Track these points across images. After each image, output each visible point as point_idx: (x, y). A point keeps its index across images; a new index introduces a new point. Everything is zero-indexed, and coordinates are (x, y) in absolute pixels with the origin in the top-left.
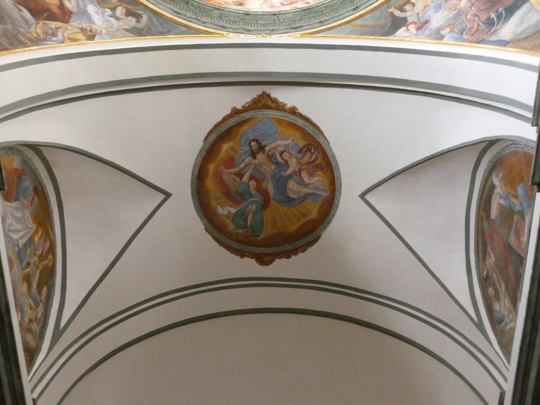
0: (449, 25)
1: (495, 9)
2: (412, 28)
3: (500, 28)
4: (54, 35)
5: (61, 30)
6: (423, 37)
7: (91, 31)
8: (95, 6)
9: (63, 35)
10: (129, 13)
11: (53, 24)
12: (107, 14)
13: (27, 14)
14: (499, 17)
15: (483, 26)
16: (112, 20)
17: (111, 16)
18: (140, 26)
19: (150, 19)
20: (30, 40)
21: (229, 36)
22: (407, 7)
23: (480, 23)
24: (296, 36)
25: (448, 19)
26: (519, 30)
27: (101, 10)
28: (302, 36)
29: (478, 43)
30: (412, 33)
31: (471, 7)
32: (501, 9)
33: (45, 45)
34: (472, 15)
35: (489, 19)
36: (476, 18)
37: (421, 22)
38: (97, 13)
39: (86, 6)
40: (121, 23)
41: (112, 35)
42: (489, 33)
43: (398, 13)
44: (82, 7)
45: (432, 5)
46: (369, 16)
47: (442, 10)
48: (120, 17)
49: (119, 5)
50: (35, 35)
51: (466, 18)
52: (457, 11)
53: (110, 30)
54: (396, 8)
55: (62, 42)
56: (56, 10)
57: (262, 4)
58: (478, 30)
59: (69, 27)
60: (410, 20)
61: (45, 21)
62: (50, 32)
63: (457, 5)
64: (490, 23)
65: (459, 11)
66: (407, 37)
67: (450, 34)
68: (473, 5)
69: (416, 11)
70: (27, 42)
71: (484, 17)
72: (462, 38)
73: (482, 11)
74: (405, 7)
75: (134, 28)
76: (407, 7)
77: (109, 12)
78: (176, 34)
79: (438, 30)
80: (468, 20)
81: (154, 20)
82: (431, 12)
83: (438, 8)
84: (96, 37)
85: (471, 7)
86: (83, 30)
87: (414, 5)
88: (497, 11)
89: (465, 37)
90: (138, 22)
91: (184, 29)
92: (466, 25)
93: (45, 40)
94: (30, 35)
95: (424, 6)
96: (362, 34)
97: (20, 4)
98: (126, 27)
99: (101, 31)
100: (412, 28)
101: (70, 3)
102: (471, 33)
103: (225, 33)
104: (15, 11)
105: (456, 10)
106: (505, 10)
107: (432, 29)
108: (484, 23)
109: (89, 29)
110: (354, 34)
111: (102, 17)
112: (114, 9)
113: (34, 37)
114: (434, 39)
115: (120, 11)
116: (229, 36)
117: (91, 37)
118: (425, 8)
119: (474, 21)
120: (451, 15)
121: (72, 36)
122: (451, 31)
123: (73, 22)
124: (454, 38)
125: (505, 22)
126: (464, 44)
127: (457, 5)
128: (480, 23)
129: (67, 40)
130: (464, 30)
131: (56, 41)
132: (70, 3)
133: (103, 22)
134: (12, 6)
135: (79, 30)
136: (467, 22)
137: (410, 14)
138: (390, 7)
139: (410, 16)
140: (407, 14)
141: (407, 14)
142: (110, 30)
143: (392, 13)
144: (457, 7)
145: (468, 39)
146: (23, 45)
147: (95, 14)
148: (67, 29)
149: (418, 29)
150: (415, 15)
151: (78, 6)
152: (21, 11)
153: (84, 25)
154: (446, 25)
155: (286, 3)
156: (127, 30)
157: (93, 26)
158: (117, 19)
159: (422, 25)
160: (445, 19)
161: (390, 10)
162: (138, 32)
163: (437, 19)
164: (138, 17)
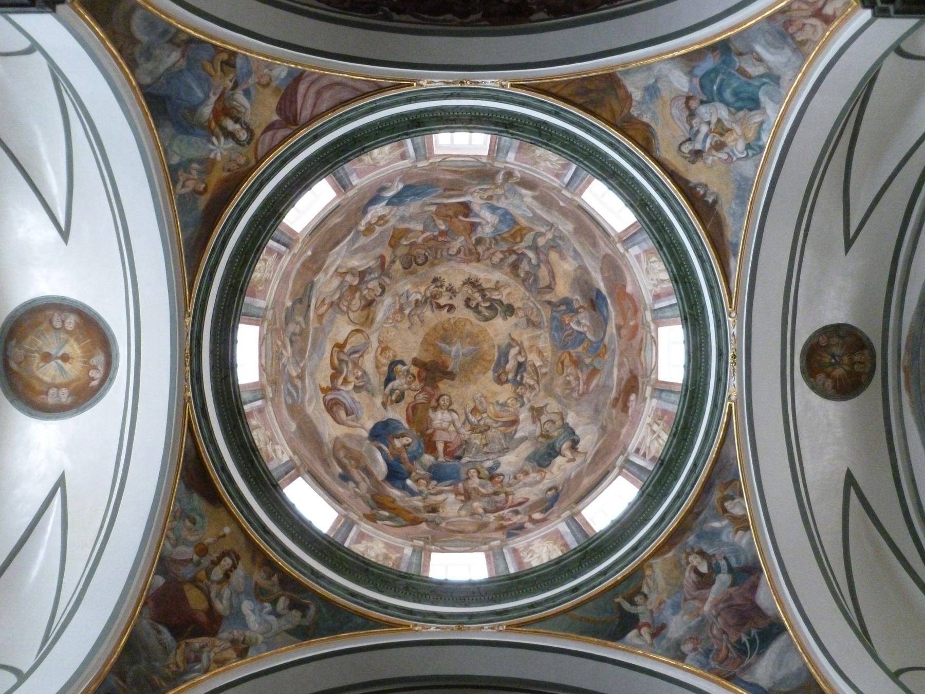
0: (691, 638)
1: (746, 628)
2: (645, 631)
3: (756, 662)
4: (198, 660)
5: (207, 649)
6: (659, 651)
7: (243, 642)
8: (252, 601)
9: (209, 656)
10: (294, 605)
11: (197, 642)
12: (265, 610)
13: (167, 635)
14: (752, 641)
15: (733, 654)
16: (272, 618)
17: (270, 613)
18: (306, 622)
19: (318, 611)
20: (167, 679)
21: (417, 628)
22: (638, 599)
23: (730, 646)
24: (501, 628)
25: (689, 628)
26: (779, 675)
27: (259, 606)
28: (510, 628)
29: (728, 679)
30: (645, 641)
31: (716, 617)
32: (754, 632)
33: (185, 681)
34: (718, 630)
35: (739, 641)
36: (724, 636)
37: (656, 625)
38: (253, 611)
39: (240, 603)
40: (282, 621)
41: (271, 645)
42: (742, 666)
43: (626, 606)
44: (235, 605)
45: (669, 601)
46: (591, 604)
47: (682, 612)
48: (282, 612)
49: (281, 595)
50: (173, 668)
51: (711, 631)
52: (700, 618)
53: (269, 635)
54: (624, 598)
55: (207, 671)
56: (203, 618)
57: (460, 509)
58: (727, 657)
59: (218, 642)
60: (643, 619)
61: (188, 641)
62: (192, 656)
63: (699, 609)
64: (742, 651)
65: (702, 621)
66: (639, 647)
67: (693, 654)
68: (719, 614)
69: (649, 607)
70: (163, 684)
71: (734, 639)
72: (708, 664)
73: (730, 626)
74: (636, 599)
75: (299, 626)
76: (638, 599)
77: (268, 606)
78: (351, 629)
79: (678, 644)
80: (714, 637)
81: (324, 610)
82: (668, 612)
83: (676, 608)
84: (250, 650)
85: (716, 617)
86: (234, 642)
87: (646, 596)
88: (748, 634)
89: (713, 664)
90: (304, 616)
91: (360, 620)
92: (713, 645)
93: (186, 672)
94: (167, 670)
95: (657, 603)
97: (160, 623)
98: (288, 626)
99: (257, 639)
100: (645, 631)
101: (221, 602)
102: (719, 659)
103: (411, 623)
104: (153, 633)
105: (698, 615)
106: (759, 634)
107: (670, 640)
108: (734, 647)
109: (242, 638)
110: (572, 631)
111: (260, 616)
112: (274, 602)
113: (173, 672)
114: (673, 659)
115: (282, 603)
116: (417, 628)
117: (242, 654)
118: (660, 604)
119: (721, 640)
120: (693, 623)
121: (219, 657)
122: (695, 649)
123: (223, 631)
124: (698, 661)
125: (761, 654)
126: (711, 676)
127: (699, 609)
128: (730, 646)
129: (213, 665)
130: (710, 651)
131: (199, 671)
132: (221, 602)
133: (260, 624)
134: (148, 627)
135: (229, 644)
136: (713, 640)
137: (641, 610)
138: (616, 595)
139: (642, 613)
140: (640, 609)
141: (640, 609)
142: (269, 635)
143: (619, 605)
144: (701, 613)
145: (715, 668)
147: (250, 613)
148: (214, 646)
149: (654, 635)
150: (648, 613)
151: (231, 605)
152: (159, 632)
154: (688, 637)
155: (490, 509)
156: (289, 632)
157: (247, 633)
158: (279, 616)
159: (658, 631)
160: (685, 628)
161: (617, 600)
162: (303, 634)
163: (677, 626)
164: (303, 608)
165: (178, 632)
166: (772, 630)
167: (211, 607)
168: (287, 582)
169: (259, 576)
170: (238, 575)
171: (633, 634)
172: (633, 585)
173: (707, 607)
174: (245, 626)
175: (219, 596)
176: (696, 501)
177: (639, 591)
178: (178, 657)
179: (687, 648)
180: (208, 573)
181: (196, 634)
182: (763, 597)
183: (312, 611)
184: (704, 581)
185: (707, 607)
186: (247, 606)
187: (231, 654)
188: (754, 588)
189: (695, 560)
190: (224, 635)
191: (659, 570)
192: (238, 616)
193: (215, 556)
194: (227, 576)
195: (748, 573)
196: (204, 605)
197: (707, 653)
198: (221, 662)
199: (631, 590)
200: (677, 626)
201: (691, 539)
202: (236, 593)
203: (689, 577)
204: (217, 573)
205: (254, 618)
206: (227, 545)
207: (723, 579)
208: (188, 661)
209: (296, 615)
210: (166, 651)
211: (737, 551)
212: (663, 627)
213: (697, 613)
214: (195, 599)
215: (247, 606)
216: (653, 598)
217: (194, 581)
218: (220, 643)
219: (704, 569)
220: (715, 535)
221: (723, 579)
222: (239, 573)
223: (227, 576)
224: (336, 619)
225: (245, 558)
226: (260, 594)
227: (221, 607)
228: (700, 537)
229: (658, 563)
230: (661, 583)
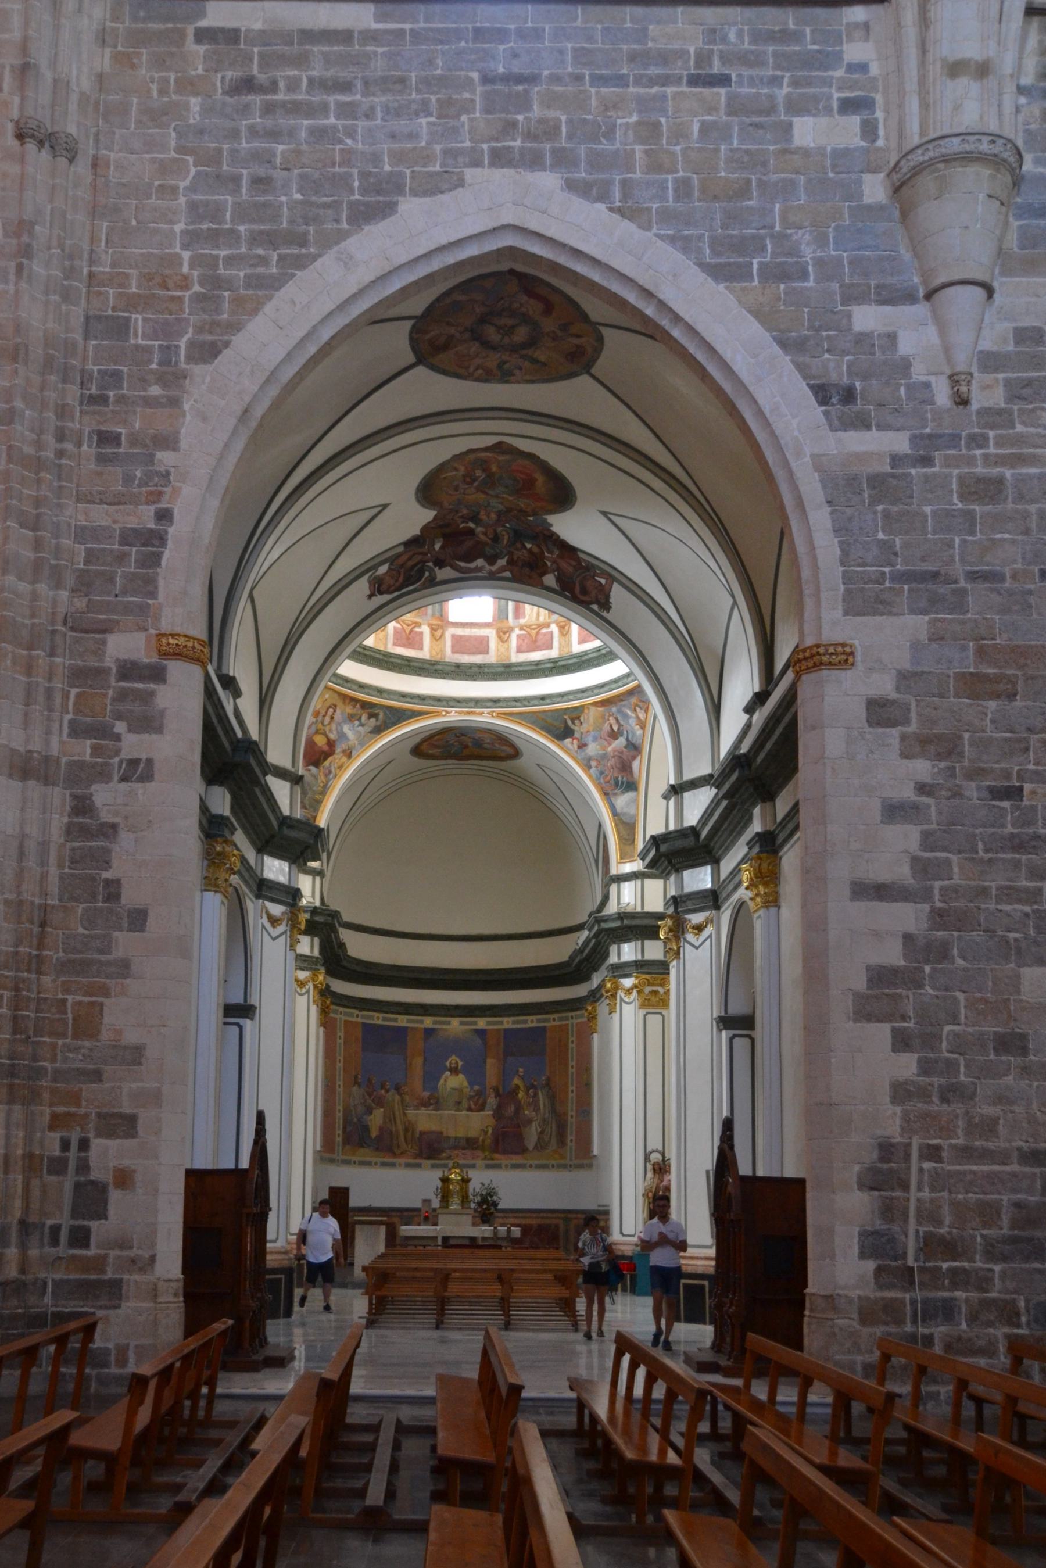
10: (371, 716)
11: (327, 763)
43: (569, 722)
56: (326, 748)
60: (576, 735)
77: (357, 723)
79: (589, 759)
83: (595, 739)
86: (344, 751)
96: (542, 728)
112: (359, 719)
125: (623, 793)
141: (576, 728)
146: (319, 802)
149: (579, 747)
153: (344, 746)
158: (362, 725)
159: (582, 746)
162: (378, 730)
163: (593, 749)
165: (317, 764)
166: (631, 786)
167: (329, 740)
168: (365, 705)
169: (349, 709)
170: (338, 716)
171: (568, 741)
172: (576, 713)
173: (610, 749)
174: (347, 739)
175: (331, 731)
176: (622, 694)
177: (578, 718)
178: (322, 778)
179: (593, 763)
180: (322, 723)
181: (325, 759)
182: (635, 765)
183: (381, 716)
184: (614, 735)
185: (610, 749)
186: (346, 728)
187: (344, 759)
188: (634, 758)
189: (612, 721)
190: (338, 750)
191: (592, 714)
192: (342, 736)
193: (323, 712)
194: (332, 718)
195: (634, 748)
196: (325, 741)
197: (602, 773)
198: (340, 767)
199: (574, 715)
200: (593, 749)
201: (614, 709)
202: (339, 724)
203: (606, 727)
204: (327, 719)
205: (350, 731)
206: (328, 704)
207: (621, 742)
208: (326, 775)
209: (373, 720)
210: (315, 777)
211: (634, 734)
212: (585, 745)
213: (604, 748)
214: (320, 741)
215: (346, 728)
216: (584, 725)
217: (317, 732)
218: (338, 758)
219: (615, 728)
220: (626, 716)
221: (621, 742)
222: (338, 711)
223: (332, 718)
224: (397, 717)
225: (340, 704)
226: (351, 718)
227: (332, 736)
228: (619, 711)
229: (593, 709)
230: (591, 720)
